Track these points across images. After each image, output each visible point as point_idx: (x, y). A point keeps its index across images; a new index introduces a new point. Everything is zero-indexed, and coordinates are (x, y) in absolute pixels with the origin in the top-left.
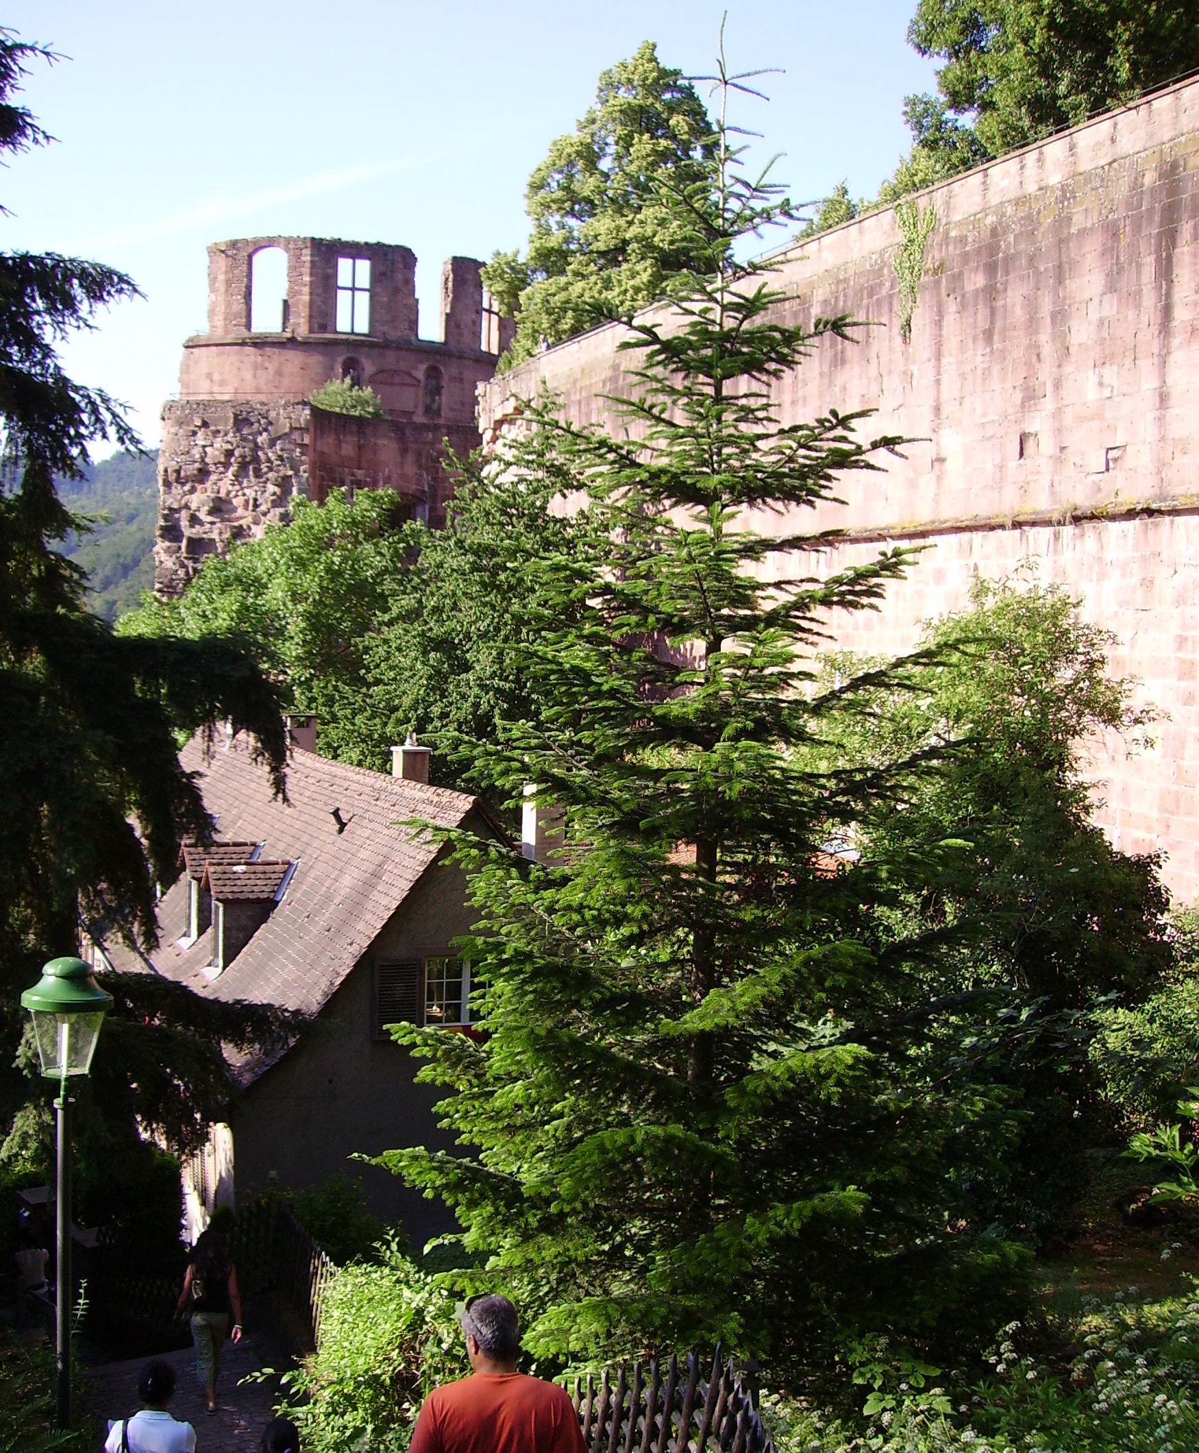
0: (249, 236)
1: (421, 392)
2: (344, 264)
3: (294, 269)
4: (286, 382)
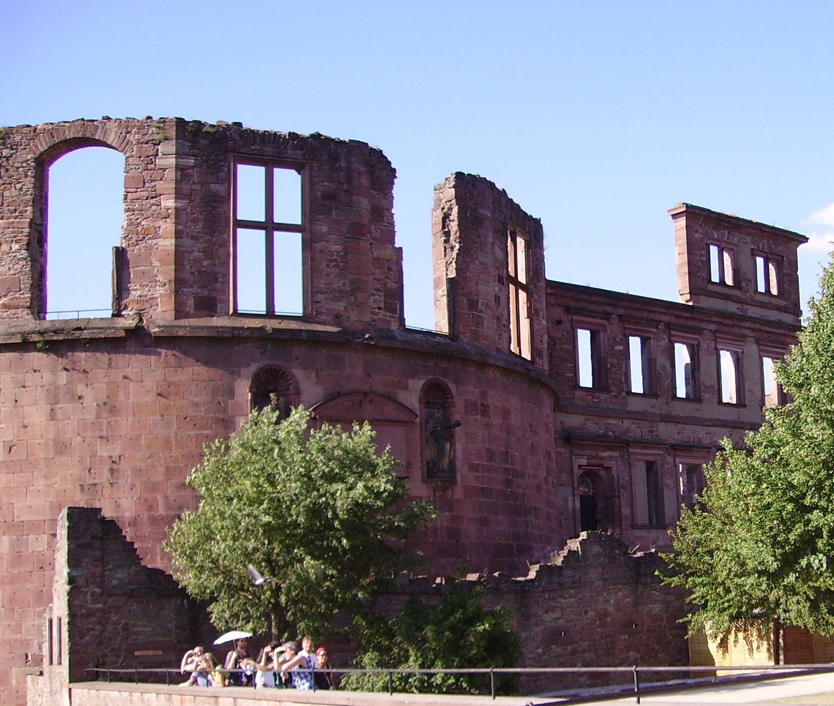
0: (38, 120)
1: (416, 434)
2: (250, 178)
3: (138, 191)
4: (125, 424)
